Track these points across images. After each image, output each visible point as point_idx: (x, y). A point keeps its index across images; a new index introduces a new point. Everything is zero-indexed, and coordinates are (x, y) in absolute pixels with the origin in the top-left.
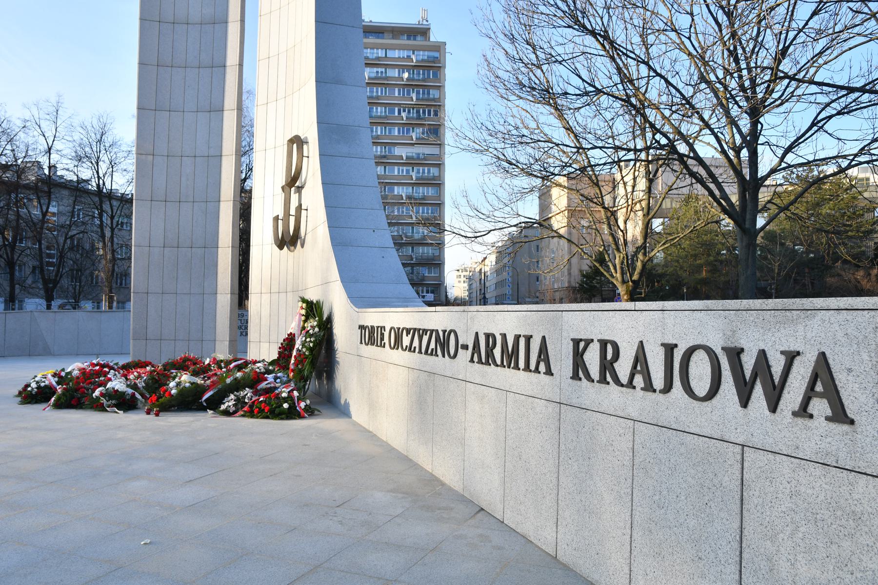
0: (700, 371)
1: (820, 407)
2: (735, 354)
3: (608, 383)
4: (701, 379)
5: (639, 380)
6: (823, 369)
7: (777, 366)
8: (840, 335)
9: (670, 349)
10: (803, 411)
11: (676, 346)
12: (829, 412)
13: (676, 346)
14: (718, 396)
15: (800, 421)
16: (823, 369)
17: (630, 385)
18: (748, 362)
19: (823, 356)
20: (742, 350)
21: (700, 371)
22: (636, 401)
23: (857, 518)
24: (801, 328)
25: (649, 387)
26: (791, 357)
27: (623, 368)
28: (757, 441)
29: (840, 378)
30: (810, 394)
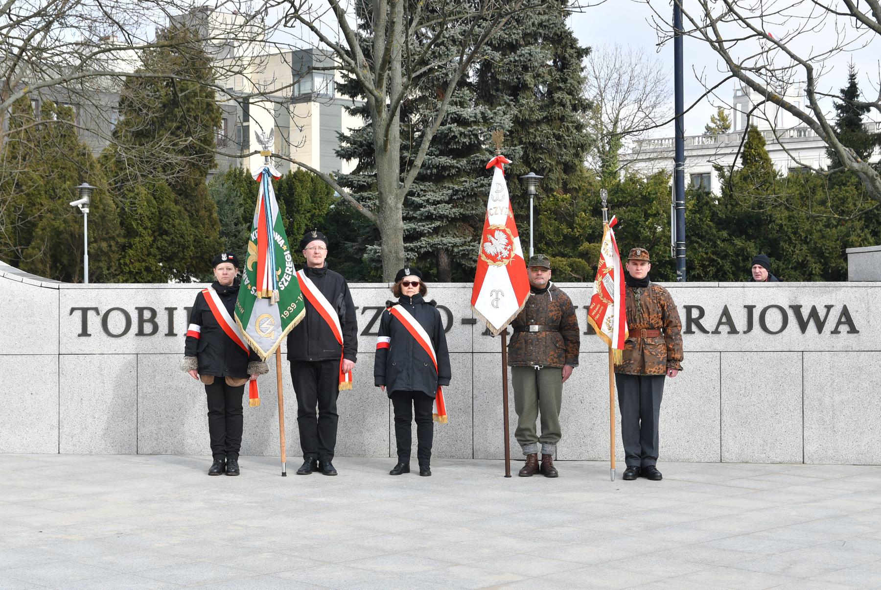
0: (774, 320)
1: (844, 328)
2: (797, 309)
3: (694, 333)
4: (774, 322)
5: (724, 329)
6: (845, 312)
7: (822, 313)
8: (852, 297)
9: (750, 309)
10: (836, 332)
11: (755, 306)
12: (848, 329)
13: (755, 306)
14: (786, 330)
15: (834, 335)
16: (845, 312)
17: (716, 332)
18: (805, 313)
19: (845, 307)
20: (801, 306)
21: (774, 320)
22: (724, 340)
23: (860, 369)
24: (834, 295)
25: (733, 331)
26: (829, 308)
27: (709, 322)
28: (811, 348)
29: (853, 315)
30: (839, 323)
